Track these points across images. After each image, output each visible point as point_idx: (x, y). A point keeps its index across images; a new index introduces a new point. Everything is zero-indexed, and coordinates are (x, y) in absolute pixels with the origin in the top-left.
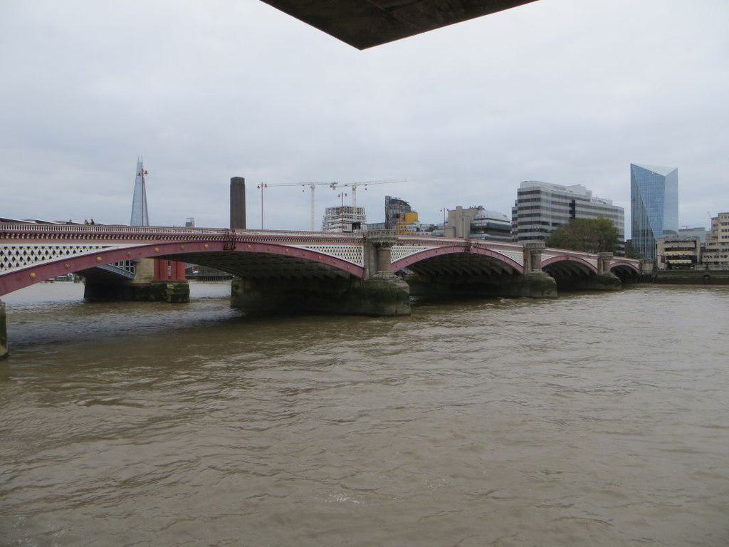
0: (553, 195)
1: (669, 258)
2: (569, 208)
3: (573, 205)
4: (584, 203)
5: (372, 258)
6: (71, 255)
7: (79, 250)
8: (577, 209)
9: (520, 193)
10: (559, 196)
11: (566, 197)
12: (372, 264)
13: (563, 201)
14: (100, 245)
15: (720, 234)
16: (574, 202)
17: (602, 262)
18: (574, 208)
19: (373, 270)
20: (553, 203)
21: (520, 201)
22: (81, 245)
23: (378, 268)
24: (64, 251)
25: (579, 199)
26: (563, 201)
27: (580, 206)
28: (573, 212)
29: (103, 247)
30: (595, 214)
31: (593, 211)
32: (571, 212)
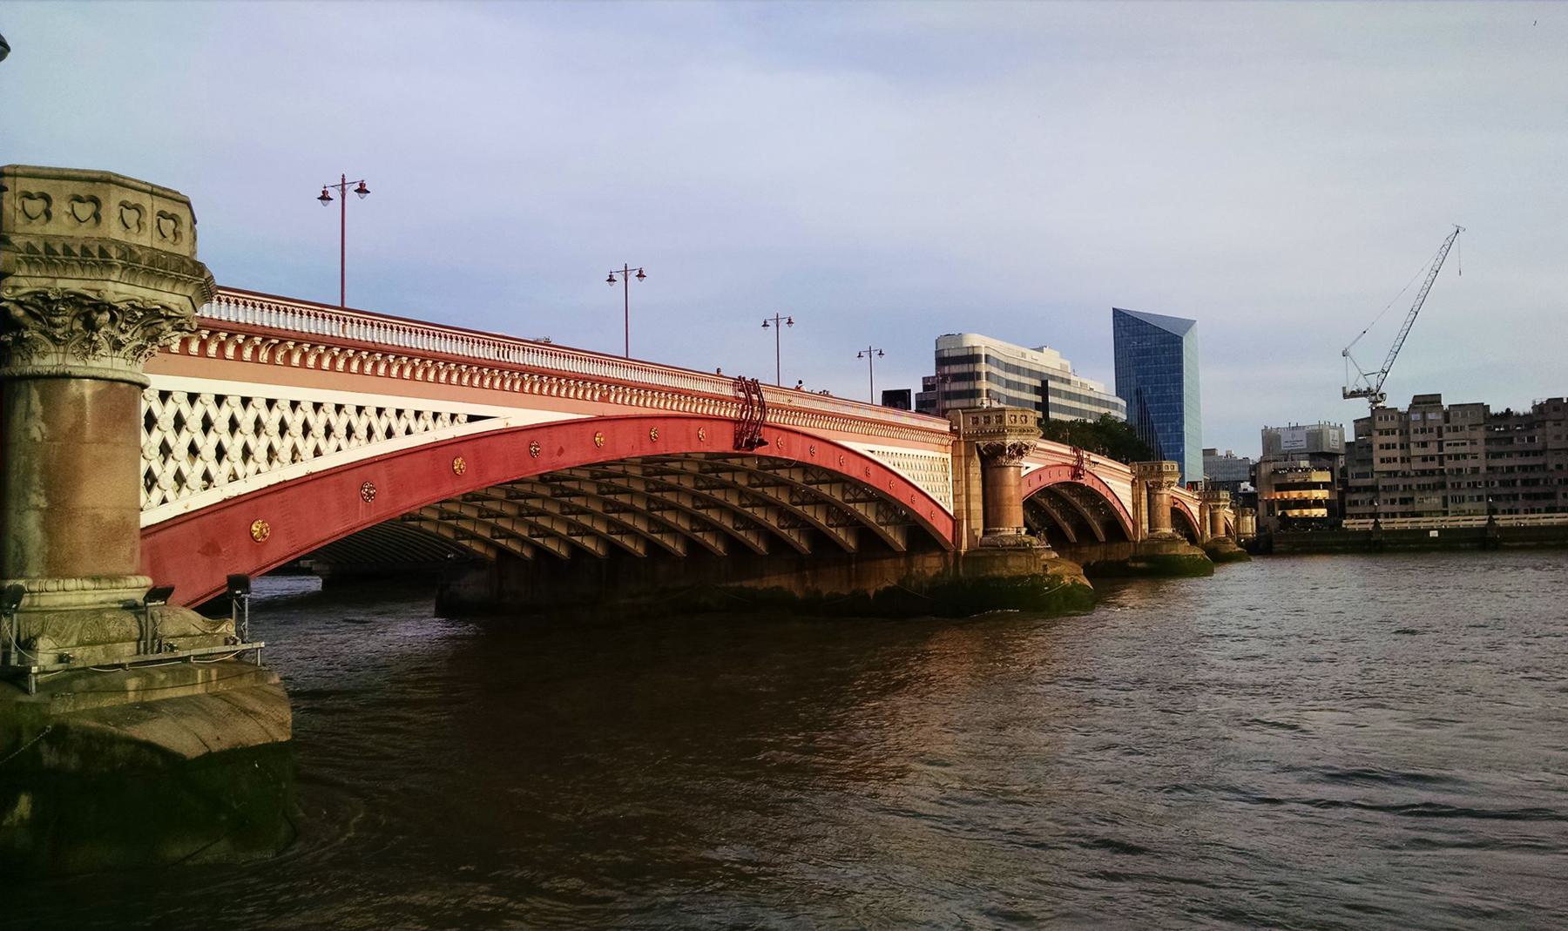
0: (1009, 368)
1: (1287, 505)
2: (1039, 399)
3: (1043, 390)
4: (1064, 387)
5: (976, 489)
6: (381, 447)
7: (403, 423)
8: (1051, 399)
9: (941, 361)
10: (1017, 370)
11: (1031, 373)
12: (977, 506)
14: (464, 409)
15: (1378, 454)
16: (1045, 383)
17: (1208, 515)
18: (1045, 399)
19: (978, 524)
21: (944, 378)
22: (410, 404)
24: (360, 427)
25: (1053, 378)
27: (1058, 393)
28: (1043, 407)
29: (471, 419)
30: (1071, 411)
32: (1038, 406)
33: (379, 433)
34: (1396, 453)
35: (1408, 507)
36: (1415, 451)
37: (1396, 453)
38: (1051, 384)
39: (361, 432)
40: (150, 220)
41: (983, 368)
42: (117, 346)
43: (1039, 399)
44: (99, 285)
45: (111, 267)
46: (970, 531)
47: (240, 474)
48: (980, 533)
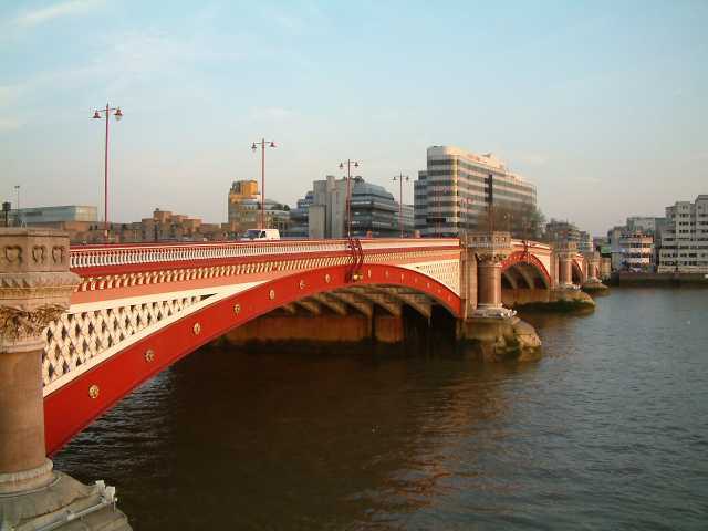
0: (470, 167)
2: (487, 186)
3: (489, 181)
4: (502, 179)
8: (494, 186)
9: (431, 163)
10: (475, 169)
11: (483, 170)
12: (474, 291)
13: (479, 175)
16: (491, 176)
18: (491, 186)
19: (474, 301)
20: (469, 177)
21: (432, 173)
22: (169, 296)
23: (483, 296)
26: (479, 175)
27: (499, 183)
29: (204, 298)
31: (519, 192)
32: (486, 190)
33: (154, 318)
34: (689, 228)
35: (693, 259)
36: (698, 227)
37: (689, 228)
38: (494, 177)
39: (144, 319)
40: (48, 254)
41: (455, 168)
42: (30, 330)
43: (487, 186)
44: (21, 303)
45: (29, 292)
46: (470, 306)
47: (82, 360)
48: (475, 307)
